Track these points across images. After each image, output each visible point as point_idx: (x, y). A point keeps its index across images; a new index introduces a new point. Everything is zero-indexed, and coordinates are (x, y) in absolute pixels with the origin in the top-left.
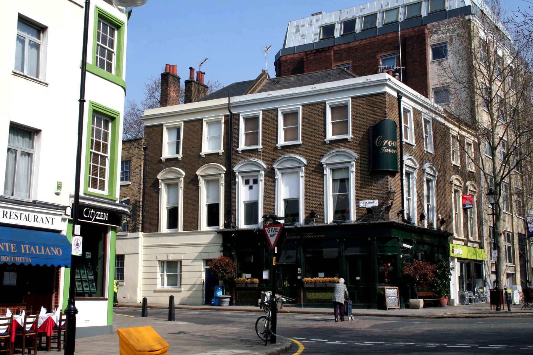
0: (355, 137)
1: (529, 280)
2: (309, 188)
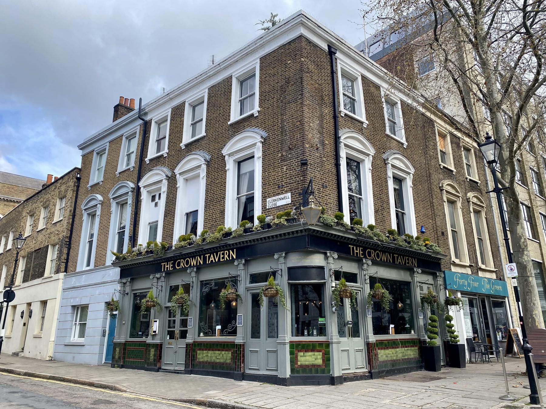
0: (263, 108)
1: (472, 89)
2: (210, 193)
